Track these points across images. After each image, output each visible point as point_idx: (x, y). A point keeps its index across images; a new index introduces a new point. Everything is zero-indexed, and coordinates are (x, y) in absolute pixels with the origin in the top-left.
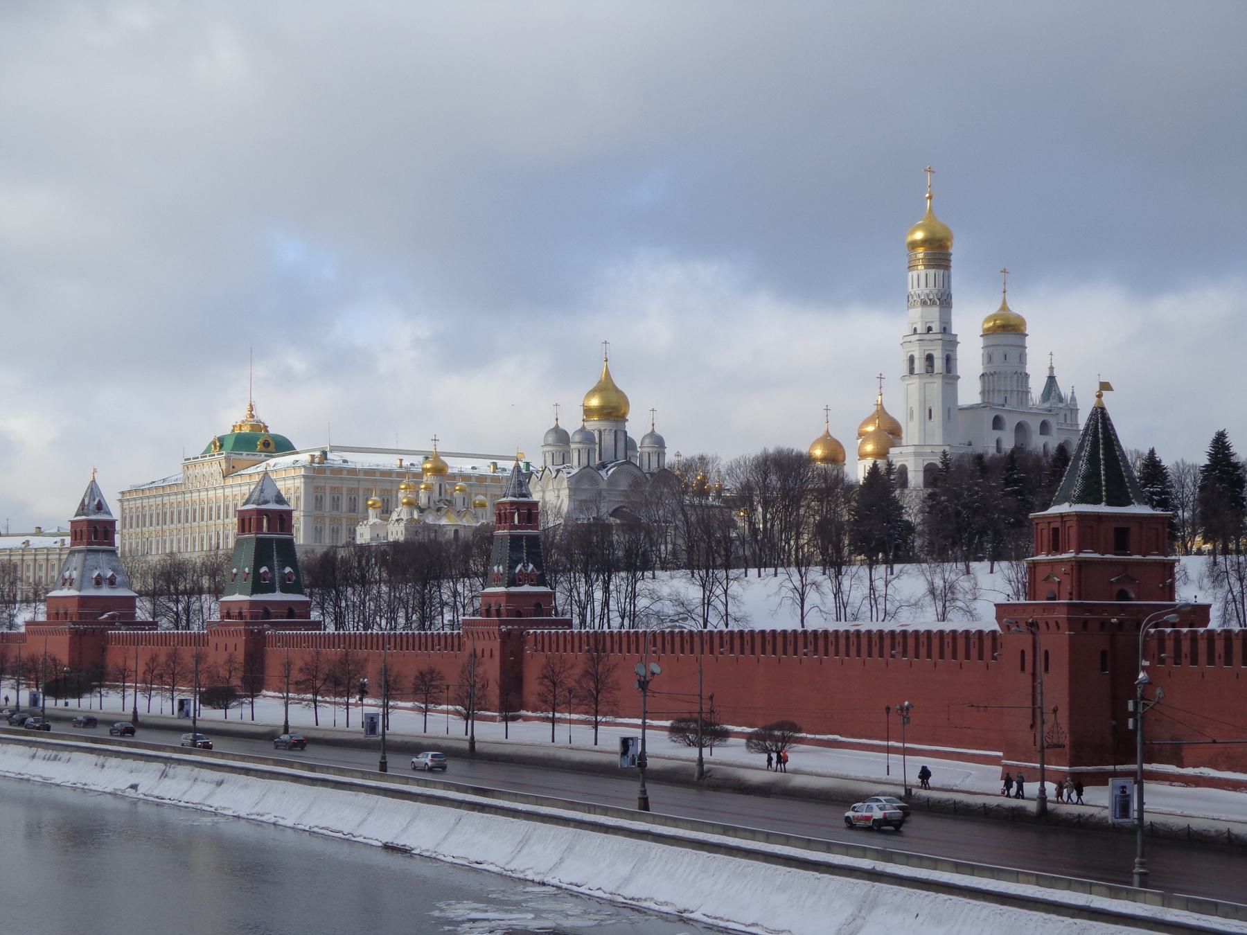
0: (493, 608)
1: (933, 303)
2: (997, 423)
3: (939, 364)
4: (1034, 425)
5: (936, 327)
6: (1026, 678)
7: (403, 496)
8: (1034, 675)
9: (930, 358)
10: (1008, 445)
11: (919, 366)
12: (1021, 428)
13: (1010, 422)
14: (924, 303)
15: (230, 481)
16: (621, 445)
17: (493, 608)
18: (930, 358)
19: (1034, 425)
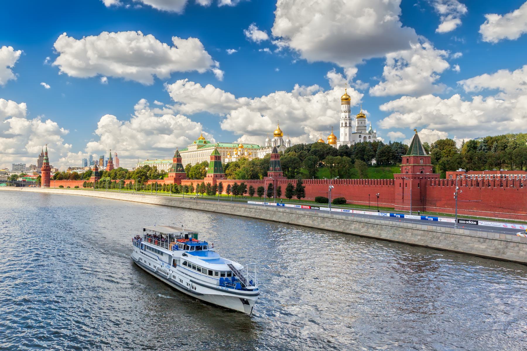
0: (271, 175)
1: (347, 112)
2: (360, 136)
3: (348, 125)
4: (367, 136)
5: (347, 117)
6: (401, 188)
7: (235, 153)
8: (403, 188)
9: (346, 123)
10: (362, 141)
11: (344, 125)
12: (365, 137)
13: (363, 136)
14: (345, 112)
15: (198, 150)
16: (282, 142)
17: (271, 175)
18: (346, 123)
19: (367, 136)
